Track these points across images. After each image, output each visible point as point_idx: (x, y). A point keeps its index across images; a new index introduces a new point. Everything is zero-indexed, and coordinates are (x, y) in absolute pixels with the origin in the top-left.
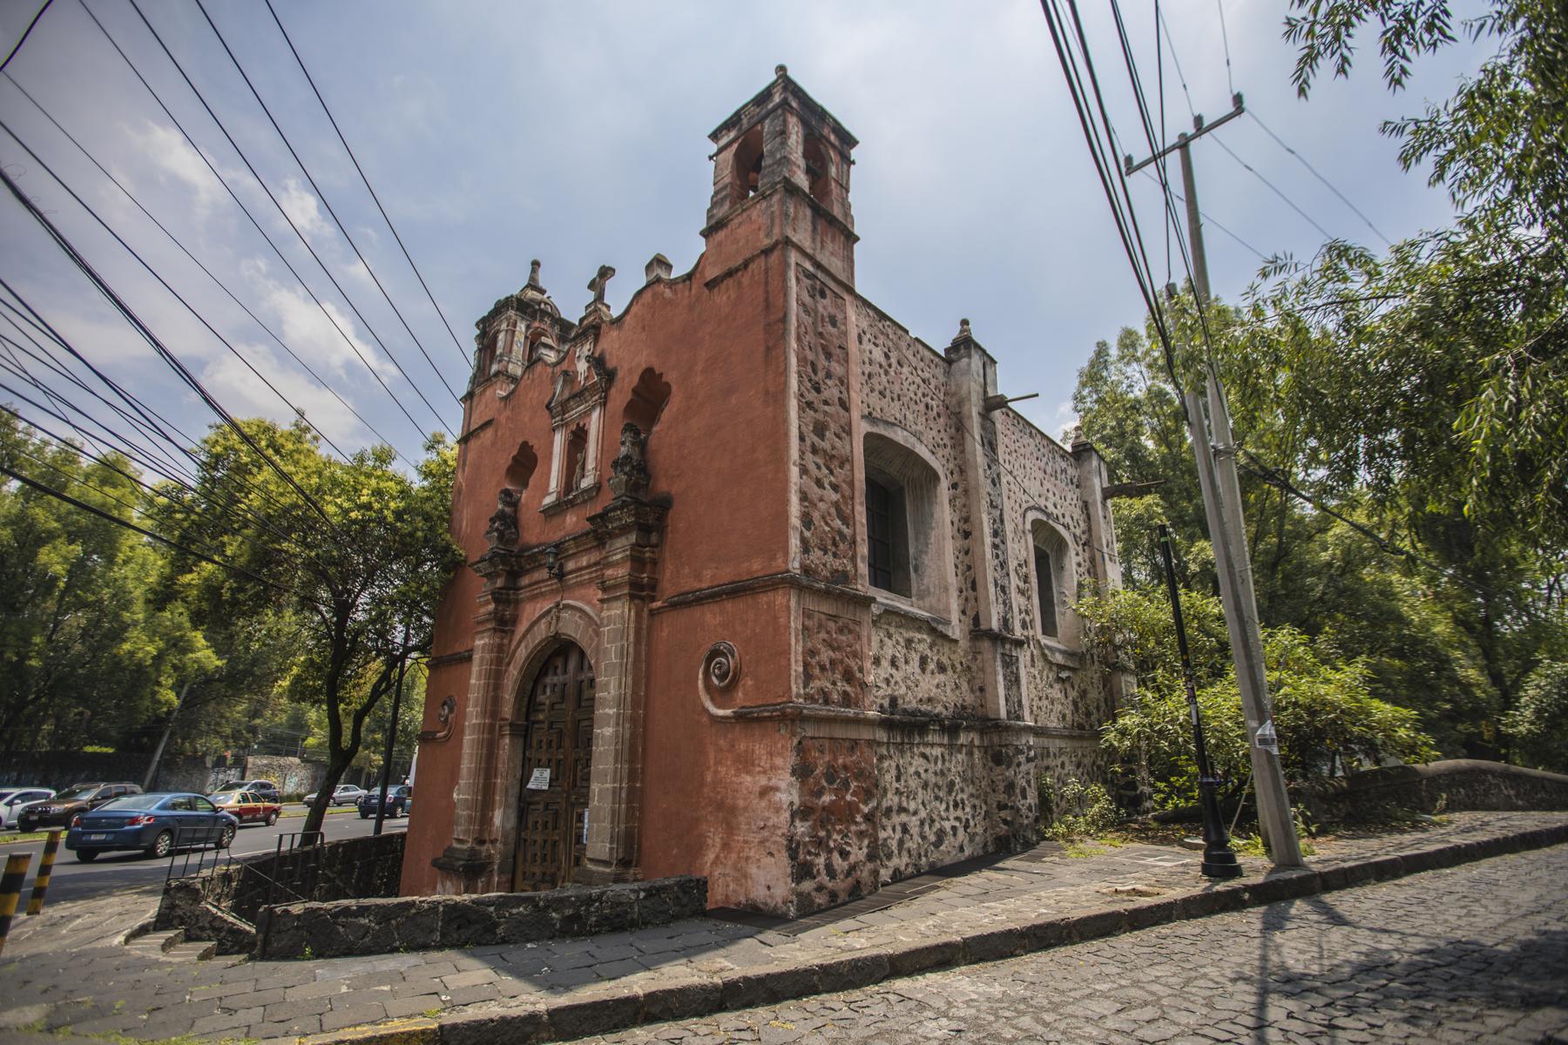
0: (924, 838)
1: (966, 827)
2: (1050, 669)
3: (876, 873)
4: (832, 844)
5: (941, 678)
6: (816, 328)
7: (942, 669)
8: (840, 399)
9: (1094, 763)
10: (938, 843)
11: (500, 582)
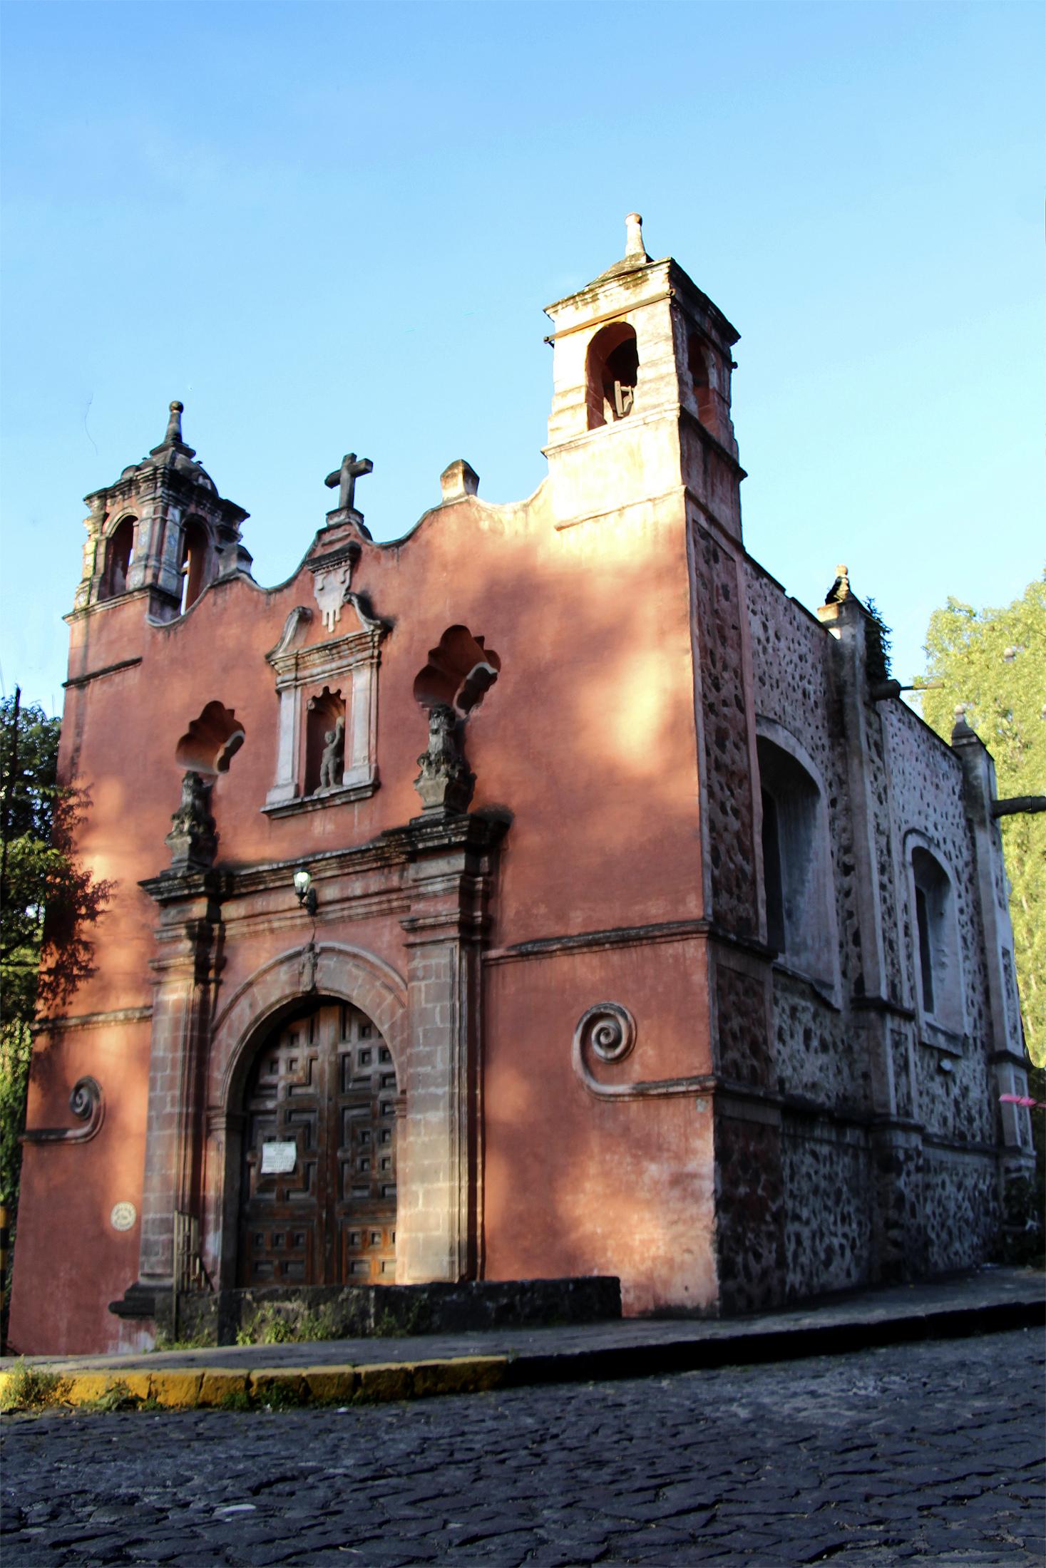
0: (815, 1253)
1: (853, 1247)
2: (932, 1055)
3: (782, 1282)
4: (747, 1243)
5: (822, 1059)
6: (712, 604)
7: (824, 1047)
8: (736, 696)
9: (976, 1186)
10: (827, 1263)
11: (199, 909)
